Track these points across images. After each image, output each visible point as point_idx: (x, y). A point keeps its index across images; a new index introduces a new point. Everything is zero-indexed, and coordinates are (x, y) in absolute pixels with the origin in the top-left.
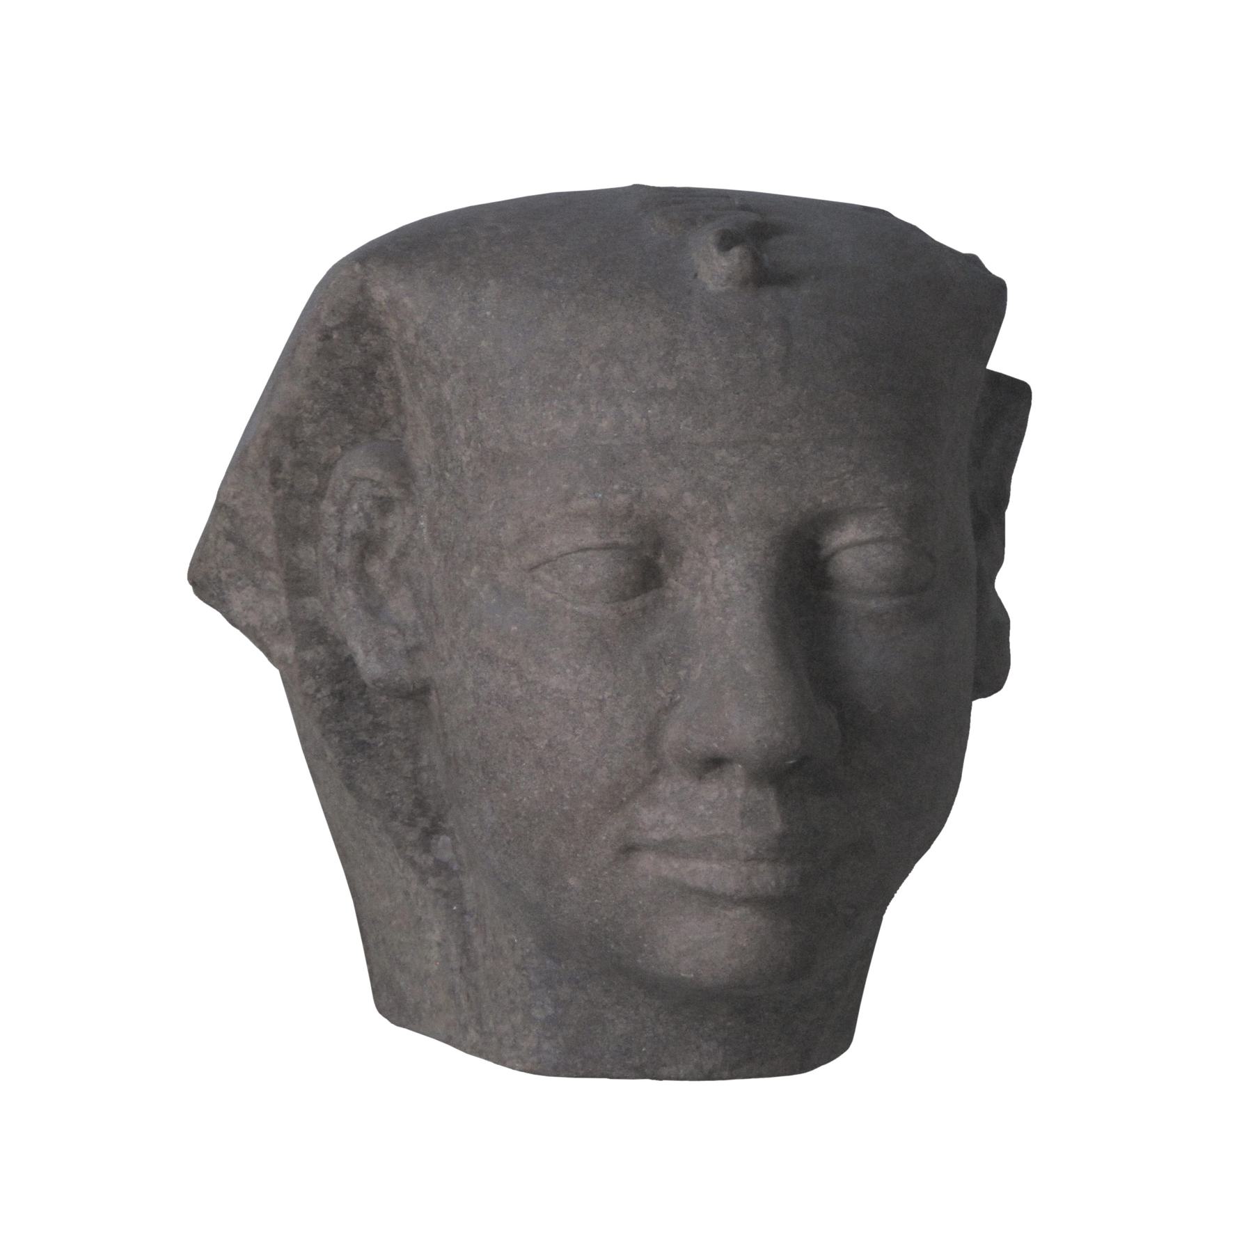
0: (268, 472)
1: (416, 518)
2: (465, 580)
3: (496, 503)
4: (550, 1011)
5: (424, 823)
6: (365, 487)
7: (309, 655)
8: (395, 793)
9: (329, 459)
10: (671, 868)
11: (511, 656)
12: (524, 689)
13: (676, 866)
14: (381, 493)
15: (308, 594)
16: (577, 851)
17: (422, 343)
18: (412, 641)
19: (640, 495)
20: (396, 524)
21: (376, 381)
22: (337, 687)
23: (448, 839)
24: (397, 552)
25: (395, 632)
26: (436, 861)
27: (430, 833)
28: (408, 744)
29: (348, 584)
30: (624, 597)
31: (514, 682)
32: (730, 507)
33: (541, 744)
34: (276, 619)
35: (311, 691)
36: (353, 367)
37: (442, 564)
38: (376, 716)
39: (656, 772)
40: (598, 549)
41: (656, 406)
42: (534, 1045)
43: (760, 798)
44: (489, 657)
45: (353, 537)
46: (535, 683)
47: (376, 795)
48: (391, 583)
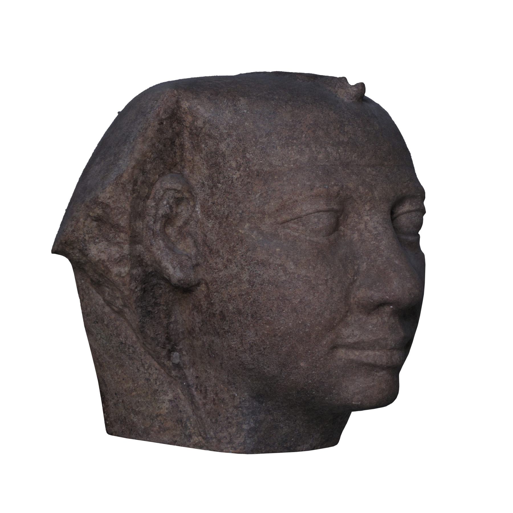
0: (131, 185)
1: (194, 206)
2: (240, 231)
3: (262, 194)
4: (252, 425)
5: (169, 347)
6: (171, 193)
7: (135, 272)
8: (159, 334)
9: (153, 181)
10: (355, 355)
11: (278, 262)
12: (288, 277)
13: (357, 354)
14: (179, 195)
15: (138, 243)
16: (309, 350)
17: (207, 125)
18: (194, 262)
19: (343, 186)
20: (184, 211)
21: (175, 146)
22: (144, 286)
23: (178, 354)
24: (183, 223)
25: (187, 258)
26: (173, 363)
27: (170, 352)
28: (167, 311)
29: (160, 238)
30: (330, 234)
31: (281, 273)
32: (376, 193)
33: (296, 301)
34: (118, 255)
35: (133, 288)
36: (168, 138)
37: (217, 226)
38: (156, 299)
39: (347, 312)
40: (324, 211)
41: (342, 148)
42: (242, 441)
43: (394, 322)
44: (263, 264)
45: (163, 216)
46: (294, 273)
47: (152, 335)
48: (178, 237)
